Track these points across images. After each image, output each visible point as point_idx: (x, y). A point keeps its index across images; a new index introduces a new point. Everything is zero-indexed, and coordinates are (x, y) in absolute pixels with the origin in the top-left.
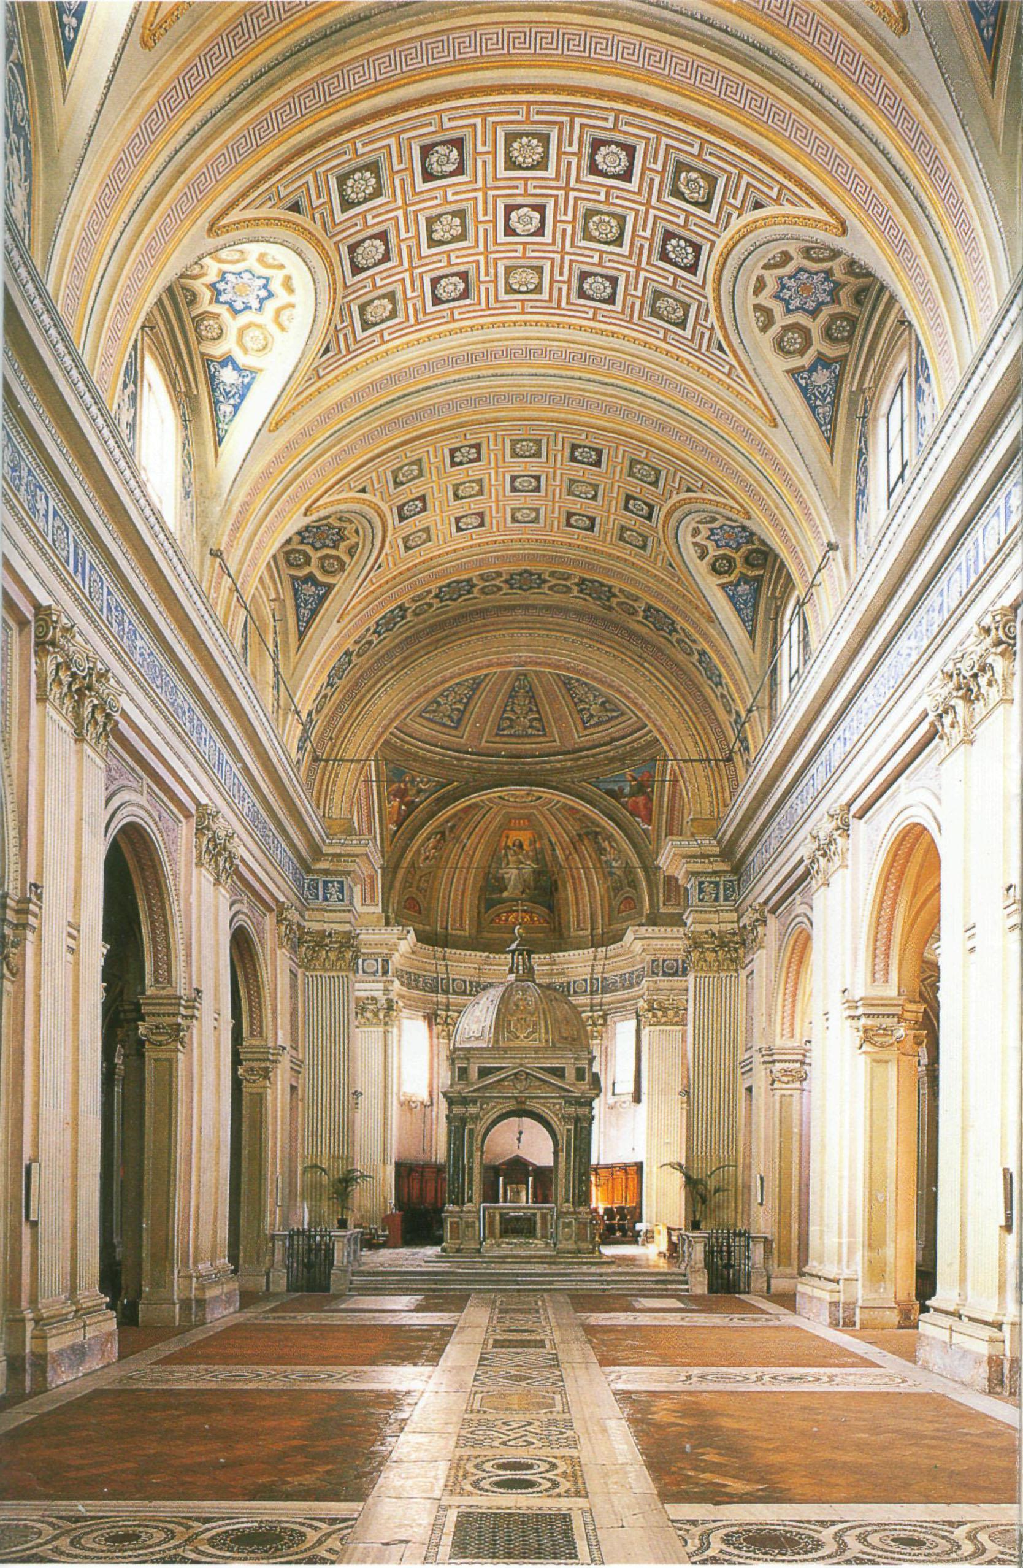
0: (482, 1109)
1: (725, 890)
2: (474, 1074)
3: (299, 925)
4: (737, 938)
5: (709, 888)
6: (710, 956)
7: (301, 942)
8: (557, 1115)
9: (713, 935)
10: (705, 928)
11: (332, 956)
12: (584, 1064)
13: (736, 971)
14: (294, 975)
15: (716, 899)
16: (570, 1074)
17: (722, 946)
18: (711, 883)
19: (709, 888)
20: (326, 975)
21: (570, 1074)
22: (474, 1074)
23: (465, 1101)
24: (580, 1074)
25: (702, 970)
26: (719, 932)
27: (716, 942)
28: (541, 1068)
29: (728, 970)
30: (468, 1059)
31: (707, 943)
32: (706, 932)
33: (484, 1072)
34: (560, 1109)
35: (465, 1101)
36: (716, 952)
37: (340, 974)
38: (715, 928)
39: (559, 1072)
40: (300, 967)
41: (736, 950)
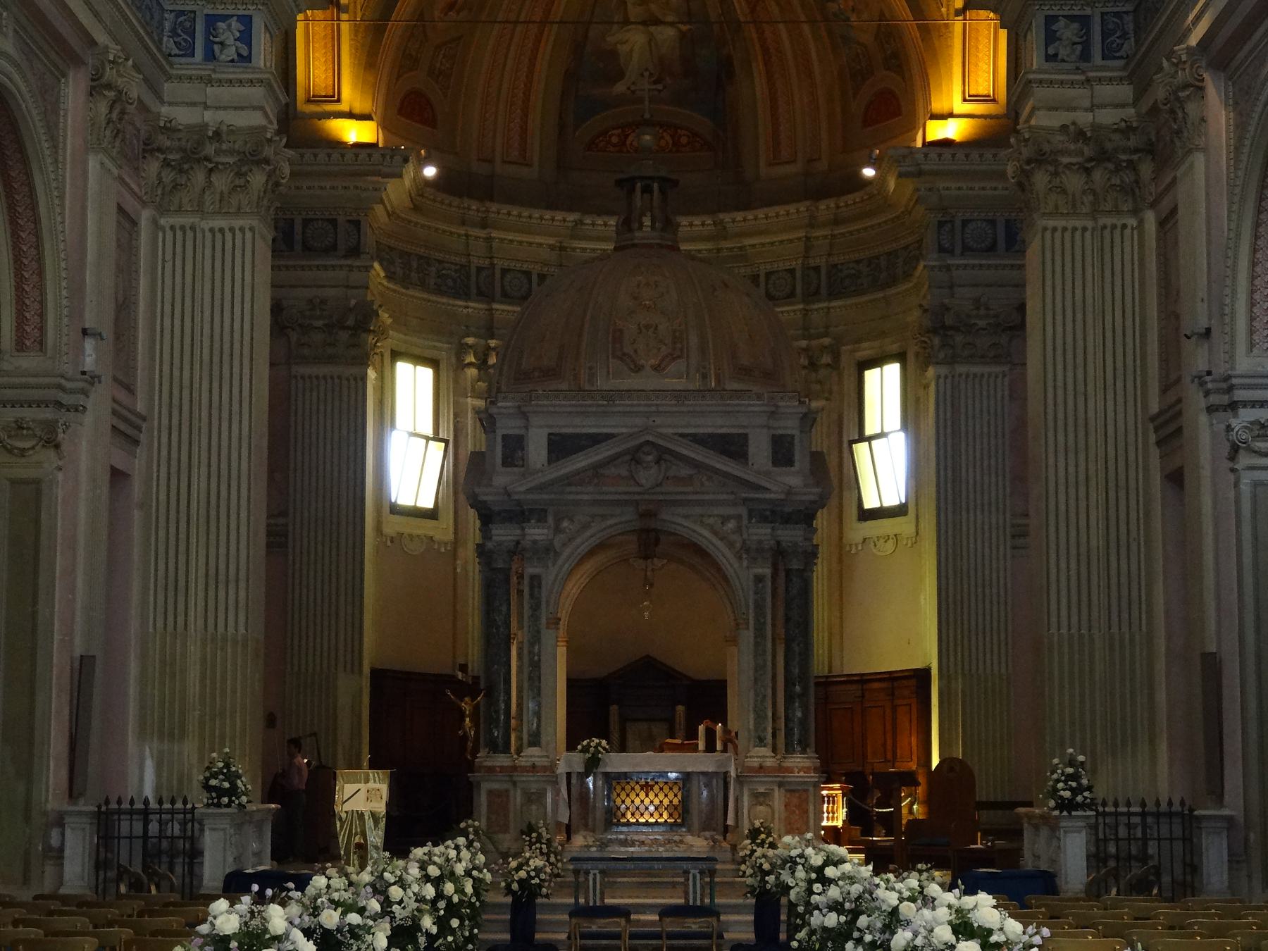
0: (558, 530)
1: (1105, 35)
2: (537, 450)
3: (143, 107)
4: (1133, 142)
5: (1068, 32)
6: (1074, 182)
7: (149, 149)
8: (731, 545)
9: (1080, 134)
10: (1064, 118)
11: (221, 182)
12: (789, 426)
13: (1135, 212)
14: (127, 220)
15: (1085, 56)
16: (760, 449)
17: (1102, 156)
18: (1072, 18)
19: (1068, 32)
20: (206, 225)
21: (760, 449)
22: (537, 450)
23: (520, 514)
24: (782, 452)
25: (1055, 213)
26: (1095, 127)
27: (1088, 151)
28: (698, 440)
29: (1117, 211)
30: (524, 415)
31: (1063, 152)
32: (1064, 128)
33: (561, 447)
34: (739, 530)
35: (520, 514)
36: (1088, 171)
37: (237, 223)
38: (1084, 119)
39: (733, 447)
40: (144, 204)
41: (1132, 166)
